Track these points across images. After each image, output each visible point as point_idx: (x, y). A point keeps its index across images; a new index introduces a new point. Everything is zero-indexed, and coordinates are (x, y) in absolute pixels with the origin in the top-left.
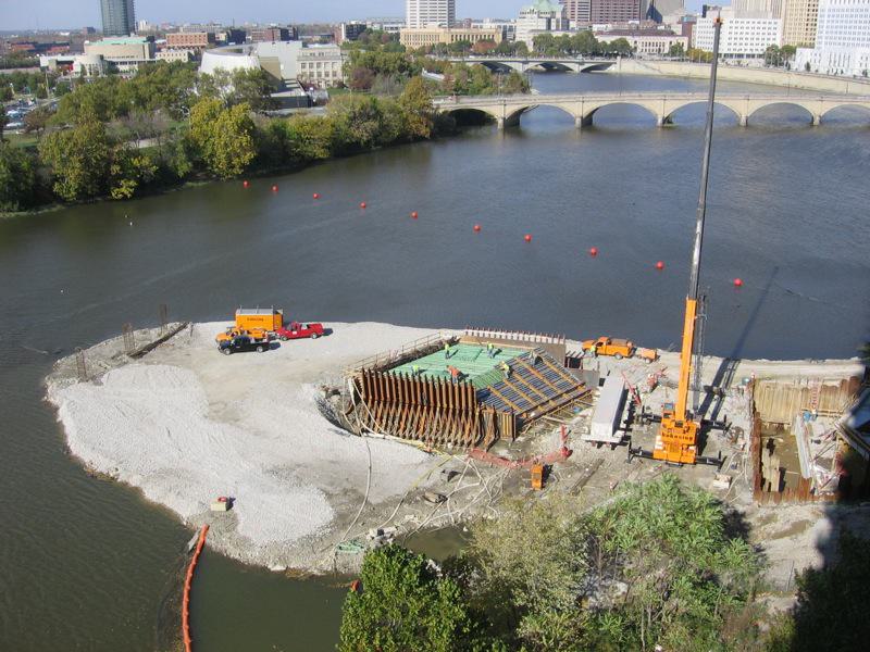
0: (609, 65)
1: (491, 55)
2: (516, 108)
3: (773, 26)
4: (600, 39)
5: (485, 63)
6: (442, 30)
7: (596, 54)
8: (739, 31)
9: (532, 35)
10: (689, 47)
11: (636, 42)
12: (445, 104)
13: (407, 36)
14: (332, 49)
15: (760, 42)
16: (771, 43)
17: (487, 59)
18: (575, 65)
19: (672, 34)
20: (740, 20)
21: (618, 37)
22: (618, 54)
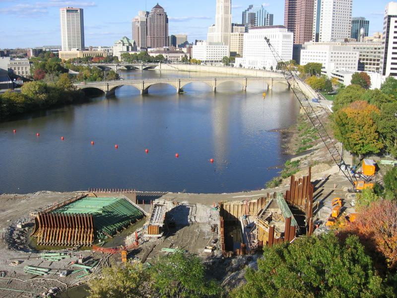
0: (156, 66)
1: (102, 63)
2: (115, 86)
3: (225, 48)
4: (151, 55)
5: (99, 67)
6: (78, 52)
7: (150, 61)
8: (211, 50)
9: (120, 54)
10: (190, 58)
11: (167, 56)
12: (80, 85)
13: (62, 55)
14: (26, 61)
15: (220, 55)
16: (225, 55)
17: (100, 64)
18: (140, 66)
19: (183, 52)
20: (211, 46)
21: (158, 54)
22: (159, 62)
